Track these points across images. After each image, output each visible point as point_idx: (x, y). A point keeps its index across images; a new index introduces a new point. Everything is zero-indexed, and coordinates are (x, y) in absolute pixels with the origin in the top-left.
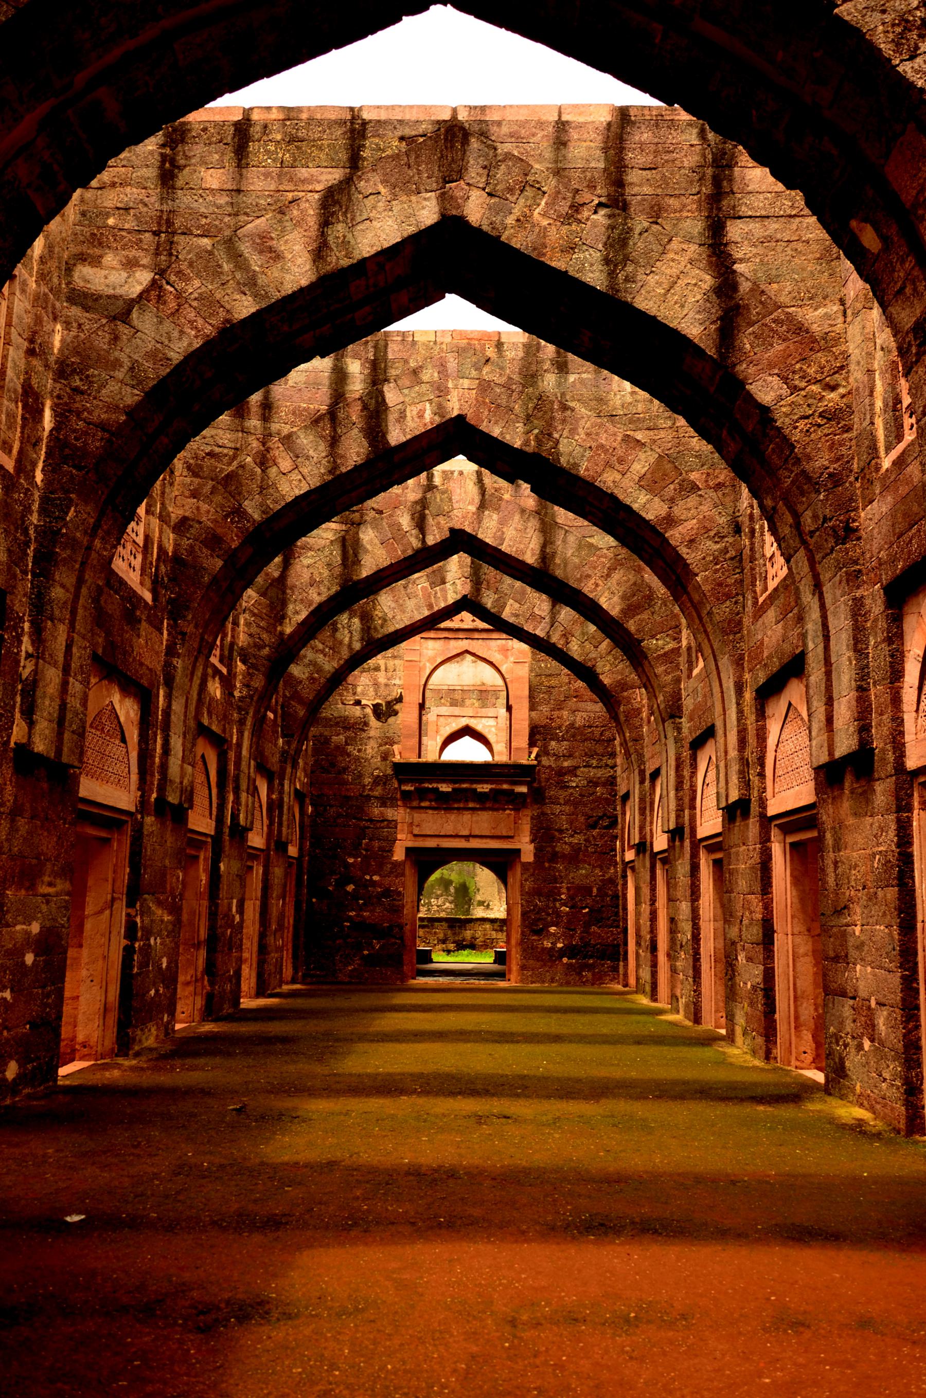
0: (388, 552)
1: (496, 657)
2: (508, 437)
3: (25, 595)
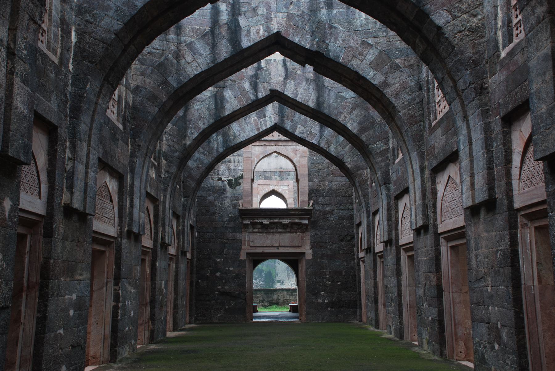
0: (238, 102)
1: (291, 155)
2: (303, 43)
3: (66, 128)
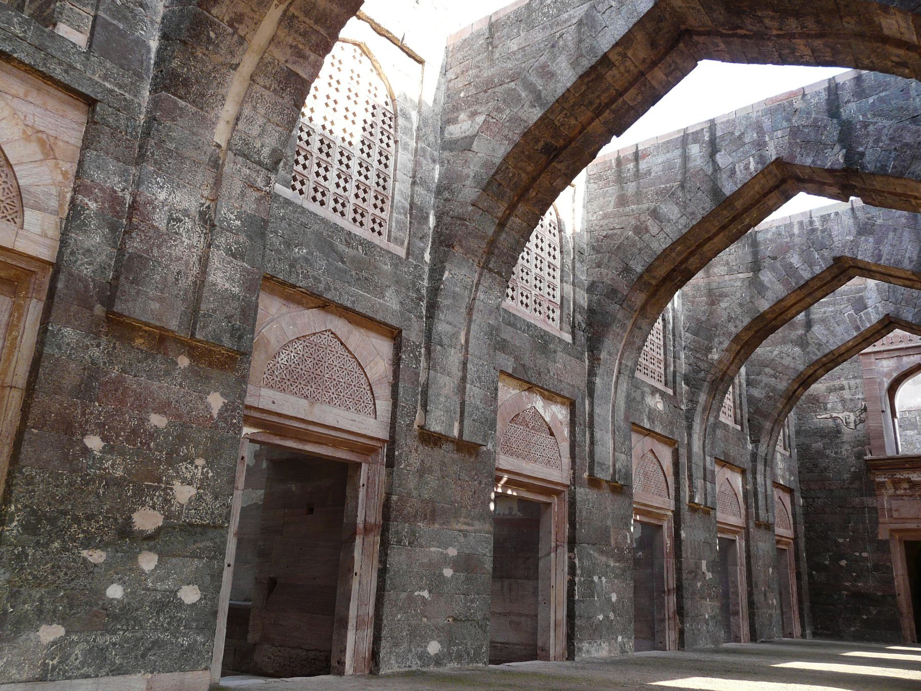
2: (819, 163)
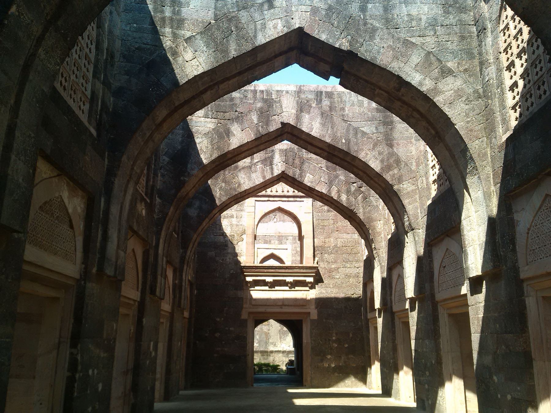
2: (331, 41)
